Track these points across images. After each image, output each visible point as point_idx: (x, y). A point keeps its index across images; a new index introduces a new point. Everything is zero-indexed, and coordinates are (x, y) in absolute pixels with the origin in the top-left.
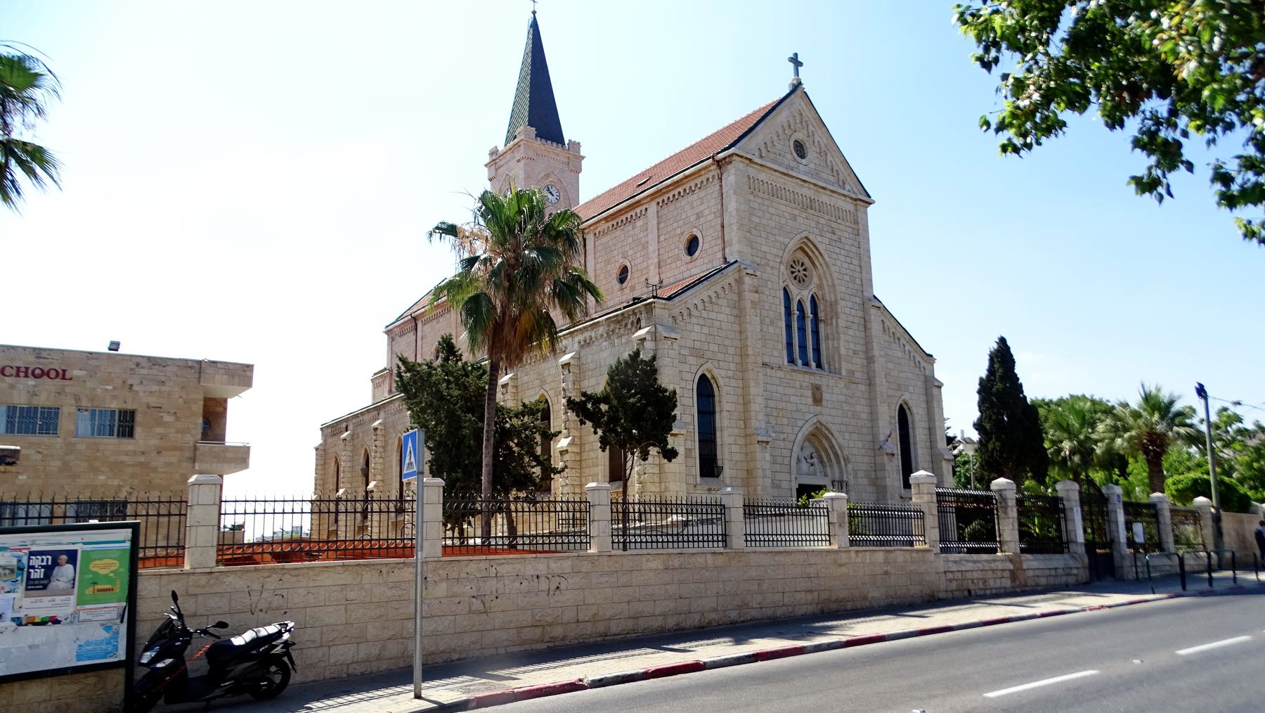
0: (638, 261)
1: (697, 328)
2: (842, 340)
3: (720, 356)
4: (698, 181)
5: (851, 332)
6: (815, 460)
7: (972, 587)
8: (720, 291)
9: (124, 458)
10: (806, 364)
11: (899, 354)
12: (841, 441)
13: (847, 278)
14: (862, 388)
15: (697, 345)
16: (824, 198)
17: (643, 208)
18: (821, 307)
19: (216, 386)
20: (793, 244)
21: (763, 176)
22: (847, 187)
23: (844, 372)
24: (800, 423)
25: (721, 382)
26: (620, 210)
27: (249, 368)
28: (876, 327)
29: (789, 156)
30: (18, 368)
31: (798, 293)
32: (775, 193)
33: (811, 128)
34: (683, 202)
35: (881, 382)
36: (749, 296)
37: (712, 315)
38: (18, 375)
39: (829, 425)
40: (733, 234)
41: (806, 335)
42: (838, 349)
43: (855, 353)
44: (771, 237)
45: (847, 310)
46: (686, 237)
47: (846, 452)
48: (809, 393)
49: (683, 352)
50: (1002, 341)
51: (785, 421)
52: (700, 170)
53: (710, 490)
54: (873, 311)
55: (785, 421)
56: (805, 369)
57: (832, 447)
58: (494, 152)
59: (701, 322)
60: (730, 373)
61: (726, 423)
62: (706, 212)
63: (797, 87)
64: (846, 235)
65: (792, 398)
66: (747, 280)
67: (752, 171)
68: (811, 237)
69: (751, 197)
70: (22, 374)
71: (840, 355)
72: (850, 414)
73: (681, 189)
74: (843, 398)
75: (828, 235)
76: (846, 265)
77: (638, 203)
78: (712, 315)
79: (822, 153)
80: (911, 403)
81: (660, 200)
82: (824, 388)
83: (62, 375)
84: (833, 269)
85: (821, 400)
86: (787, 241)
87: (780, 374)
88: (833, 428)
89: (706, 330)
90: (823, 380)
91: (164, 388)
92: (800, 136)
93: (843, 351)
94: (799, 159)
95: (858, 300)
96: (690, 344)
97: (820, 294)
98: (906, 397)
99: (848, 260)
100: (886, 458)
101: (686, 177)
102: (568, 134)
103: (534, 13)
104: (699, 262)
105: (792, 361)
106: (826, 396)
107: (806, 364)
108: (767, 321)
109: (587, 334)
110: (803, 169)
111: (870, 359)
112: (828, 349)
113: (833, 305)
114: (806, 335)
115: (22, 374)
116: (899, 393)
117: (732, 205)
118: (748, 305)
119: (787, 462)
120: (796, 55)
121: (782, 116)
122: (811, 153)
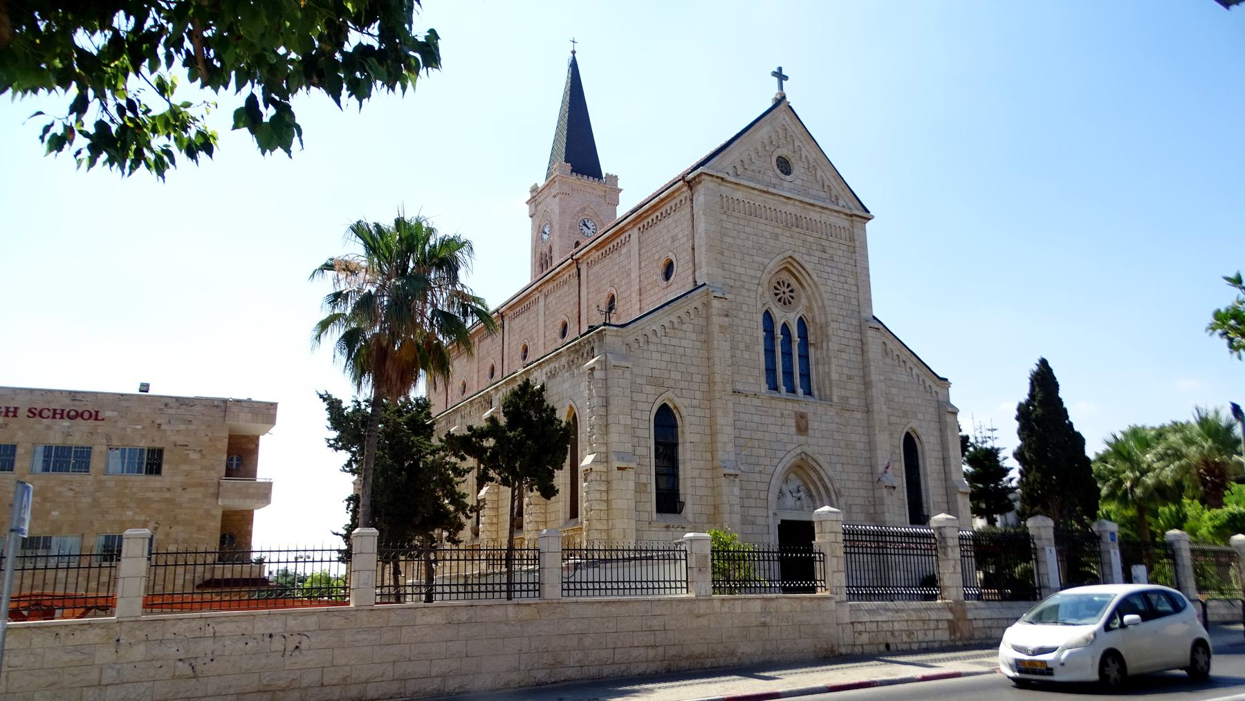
0: (623, 288)
1: (656, 356)
2: (833, 363)
3: (683, 385)
4: (673, 204)
5: (844, 356)
6: (802, 494)
7: (890, 640)
8: (683, 316)
9: (148, 494)
10: (792, 390)
11: (905, 378)
12: (831, 473)
13: (840, 298)
14: (858, 415)
15: (656, 373)
16: (814, 215)
17: (626, 235)
18: (811, 330)
19: (244, 424)
20: (773, 264)
21: (738, 195)
22: (841, 202)
23: (835, 399)
24: (780, 454)
25: (684, 413)
26: (608, 238)
27: (274, 406)
28: (874, 350)
29: (771, 173)
30: (55, 410)
31: (781, 316)
32: (753, 212)
33: (797, 143)
34: (661, 225)
35: (881, 409)
36: (717, 320)
37: (675, 342)
38: (54, 417)
39: (816, 456)
40: (701, 255)
41: (789, 359)
42: (828, 374)
43: (850, 378)
44: (747, 259)
45: (841, 333)
46: (663, 261)
47: (837, 485)
48: (792, 422)
49: (639, 380)
50: (1044, 363)
51: (762, 452)
52: (673, 192)
53: (668, 527)
54: (871, 333)
55: (762, 452)
56: (791, 396)
57: (821, 479)
58: (534, 190)
59: (661, 349)
60: (695, 402)
61: (688, 455)
62: (680, 235)
63: (780, 101)
64: (840, 253)
65: (771, 428)
66: (715, 303)
67: (725, 190)
68: (797, 257)
69: (724, 217)
70: (11, 414)
71: (830, 381)
72: (843, 444)
73: (658, 213)
74: (834, 426)
75: (818, 254)
76: (840, 285)
77: (622, 230)
78: (675, 342)
79: (811, 168)
80: (919, 431)
81: (641, 225)
82: (810, 416)
83: (95, 416)
84: (822, 288)
85: (807, 429)
86: (766, 261)
87: (756, 402)
88: (821, 460)
89: (666, 357)
90: (810, 407)
91: (192, 427)
92: (783, 152)
93: (834, 376)
94: (782, 176)
95: (854, 322)
96: (647, 372)
97: (809, 316)
98: (914, 424)
99: (842, 279)
100: (885, 491)
101: (662, 200)
102: (605, 170)
103: (574, 52)
104: (674, 287)
105: (774, 387)
106: (813, 425)
107: (792, 390)
108: (742, 346)
109: (552, 365)
110: (787, 185)
111: (867, 385)
112: (818, 372)
113: (823, 327)
114: (789, 359)
115: (11, 414)
116: (904, 421)
117: (701, 227)
118: (716, 329)
119: (763, 495)
120: (780, 69)
121: (763, 132)
122: (798, 170)
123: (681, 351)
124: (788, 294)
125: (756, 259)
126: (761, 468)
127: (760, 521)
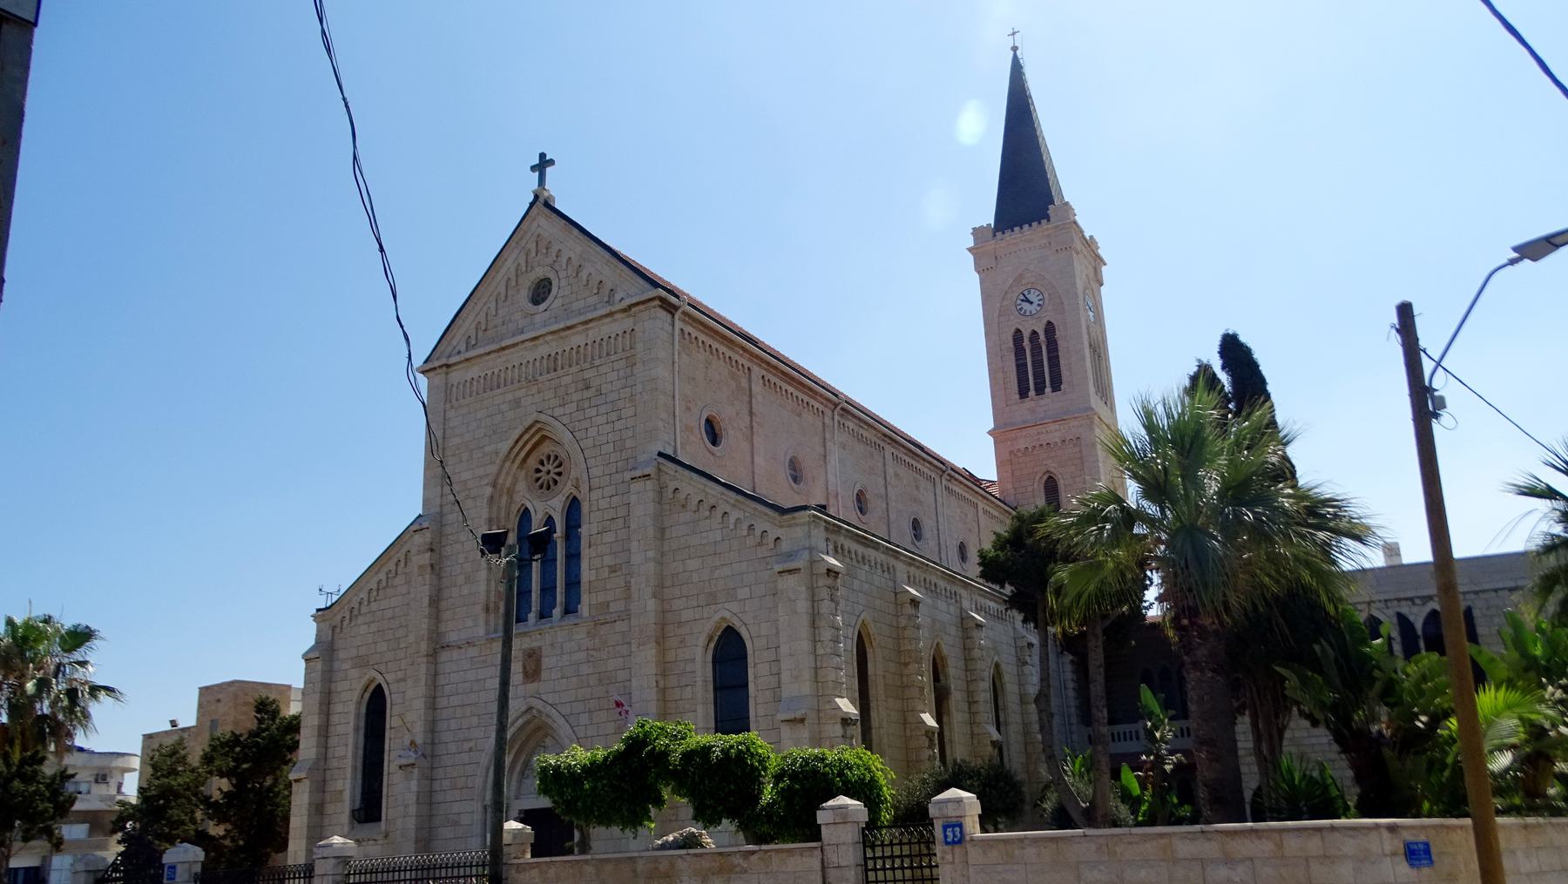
15: (362, 651)
16: (577, 340)
87: (472, 652)
89: (374, 628)
96: (354, 652)
99: (613, 416)
103: (1015, 49)
123: (389, 613)
124: (544, 469)
125: (487, 449)
126: (472, 744)
127: (465, 820)
